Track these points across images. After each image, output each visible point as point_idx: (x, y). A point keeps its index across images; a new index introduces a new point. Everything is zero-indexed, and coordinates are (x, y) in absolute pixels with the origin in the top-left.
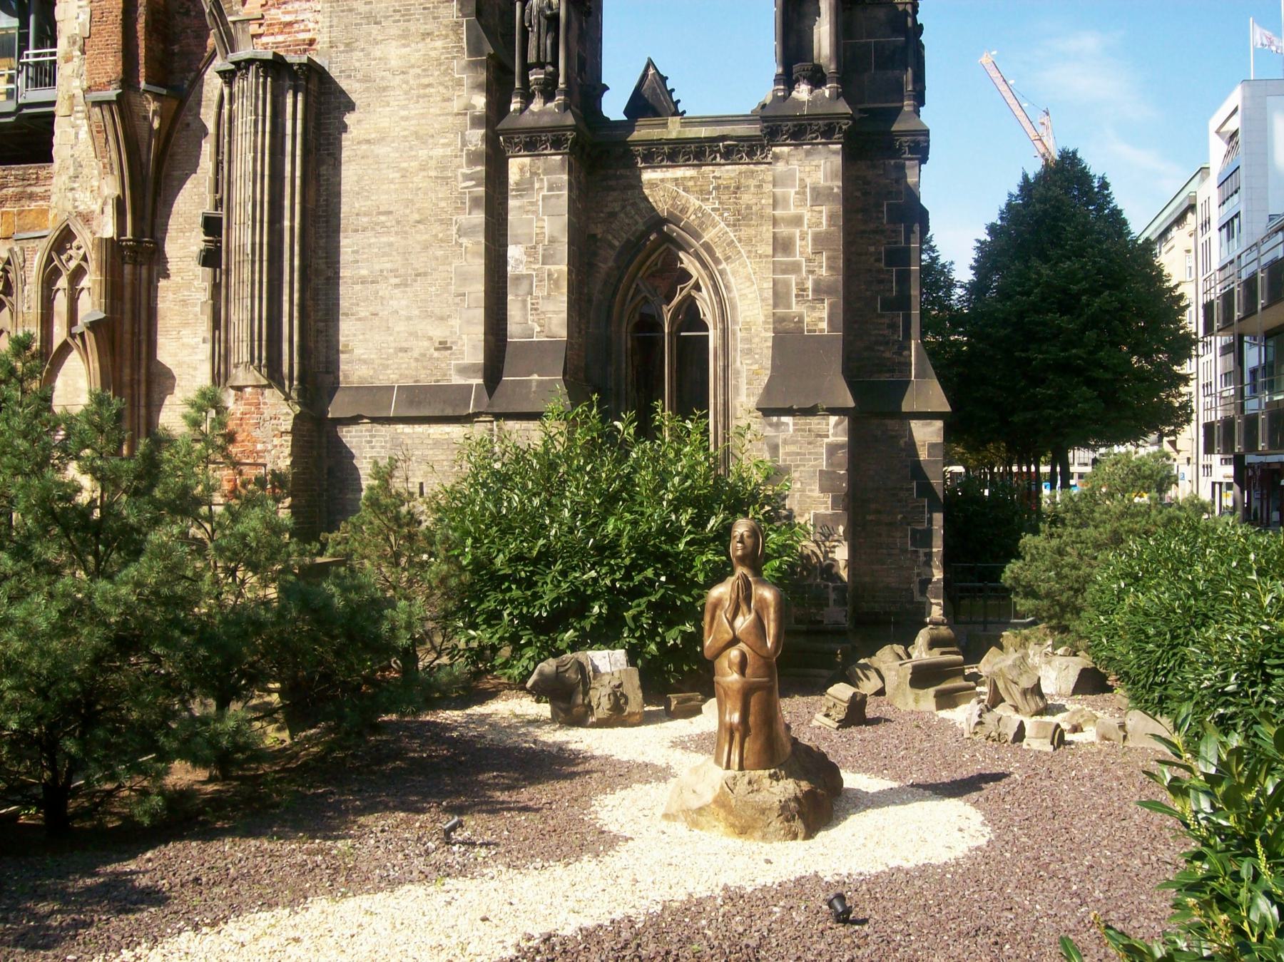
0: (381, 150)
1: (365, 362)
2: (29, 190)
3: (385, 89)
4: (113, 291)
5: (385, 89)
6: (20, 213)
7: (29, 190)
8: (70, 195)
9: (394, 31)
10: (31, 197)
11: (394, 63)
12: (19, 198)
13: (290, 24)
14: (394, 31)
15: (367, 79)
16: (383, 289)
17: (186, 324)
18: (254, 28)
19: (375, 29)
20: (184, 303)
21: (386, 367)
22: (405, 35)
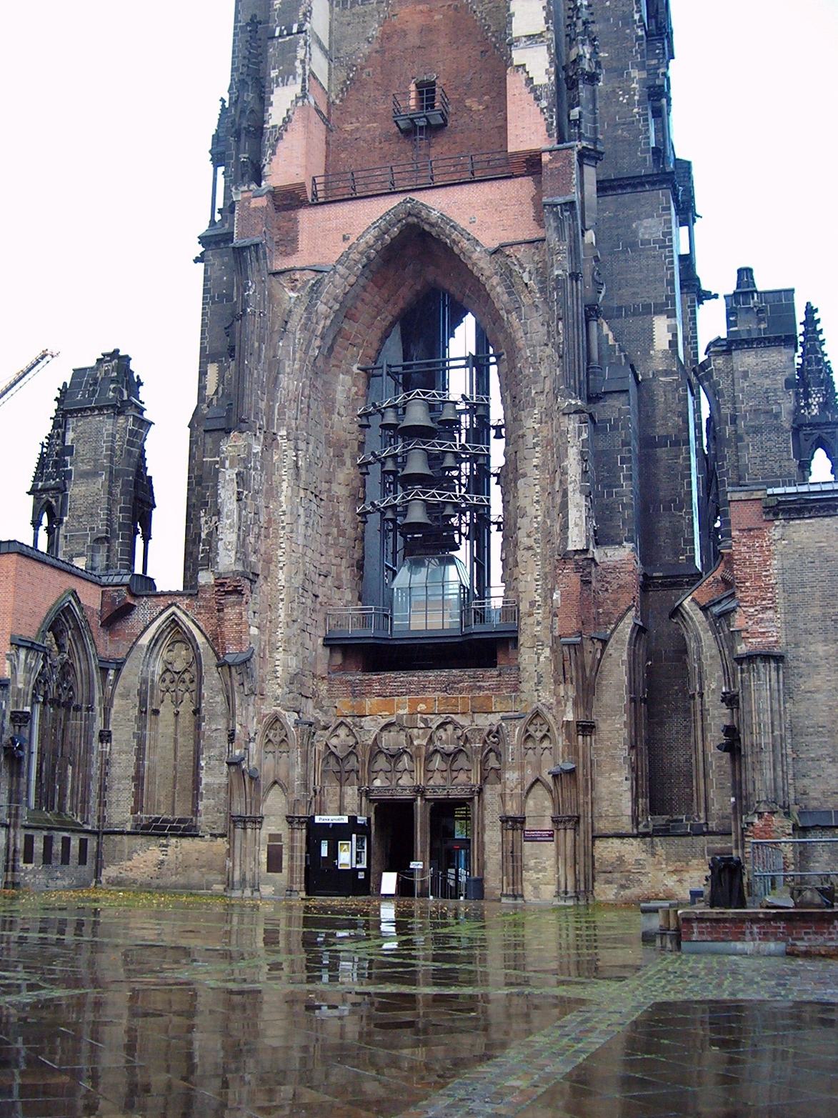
0: (817, 696)
1: (816, 799)
2: (478, 684)
3: (817, 666)
4: (573, 750)
5: (817, 666)
6: (473, 698)
7: (478, 684)
8: (536, 693)
9: (821, 638)
10: (480, 688)
11: (821, 654)
12: (471, 689)
13: (764, 633)
14: (821, 638)
15: (807, 661)
16: (823, 764)
17: (614, 770)
18: (744, 634)
19: (810, 637)
20: (613, 757)
21: (827, 802)
22: (825, 640)
